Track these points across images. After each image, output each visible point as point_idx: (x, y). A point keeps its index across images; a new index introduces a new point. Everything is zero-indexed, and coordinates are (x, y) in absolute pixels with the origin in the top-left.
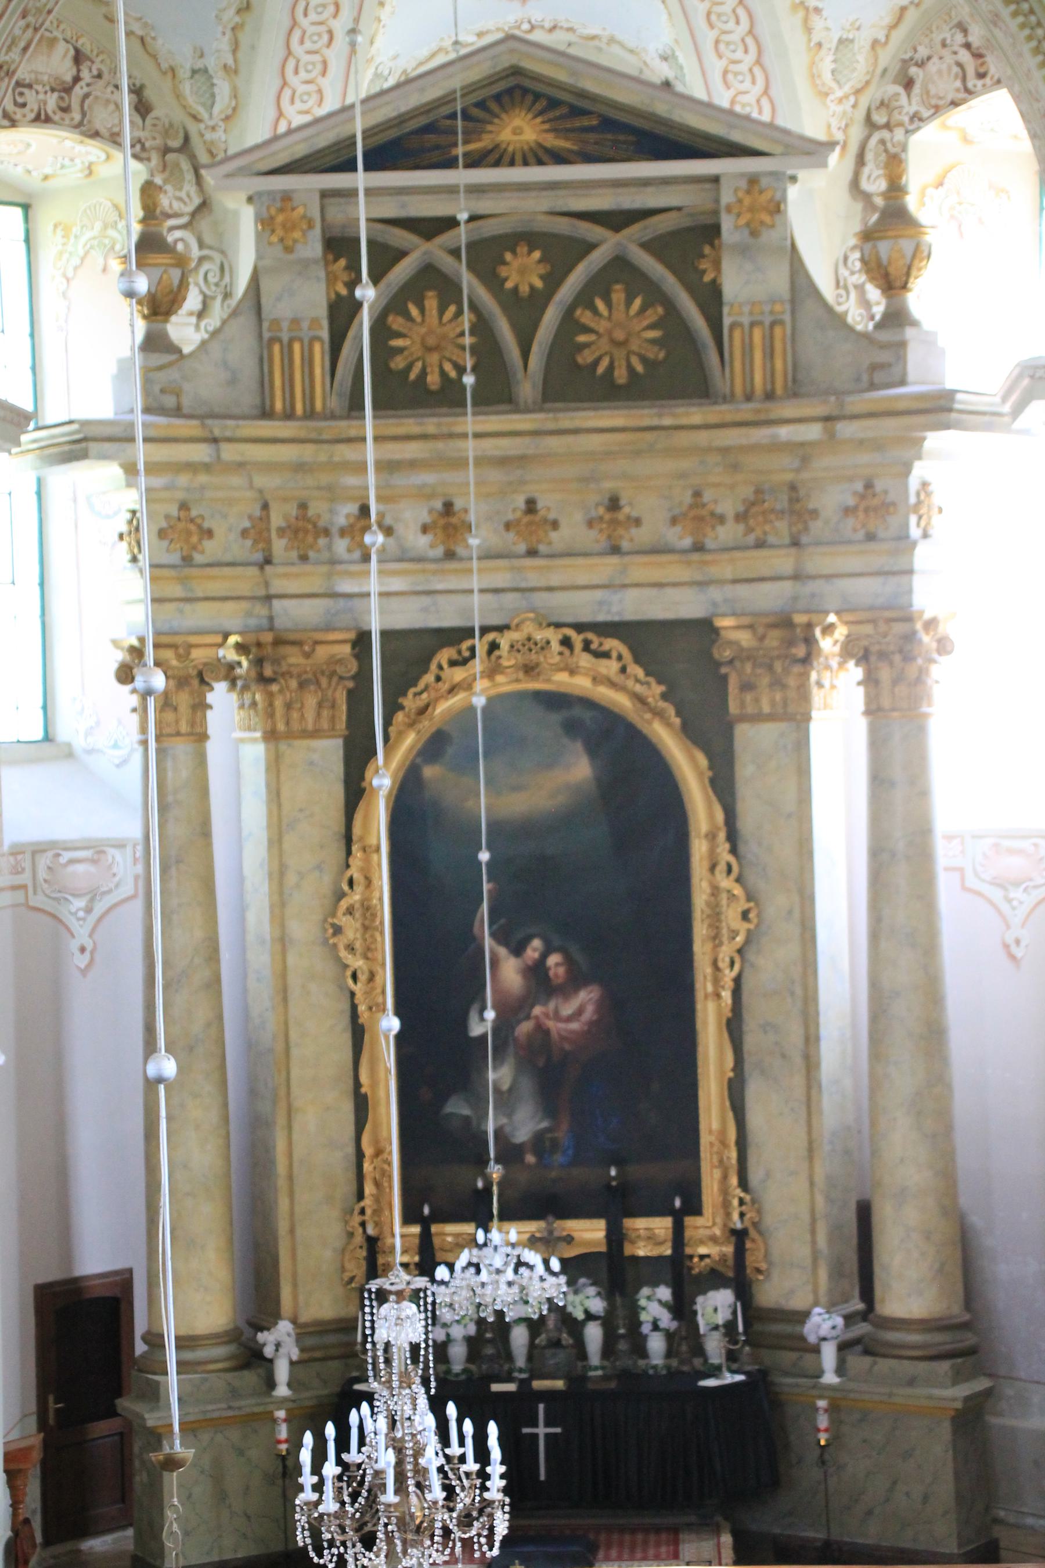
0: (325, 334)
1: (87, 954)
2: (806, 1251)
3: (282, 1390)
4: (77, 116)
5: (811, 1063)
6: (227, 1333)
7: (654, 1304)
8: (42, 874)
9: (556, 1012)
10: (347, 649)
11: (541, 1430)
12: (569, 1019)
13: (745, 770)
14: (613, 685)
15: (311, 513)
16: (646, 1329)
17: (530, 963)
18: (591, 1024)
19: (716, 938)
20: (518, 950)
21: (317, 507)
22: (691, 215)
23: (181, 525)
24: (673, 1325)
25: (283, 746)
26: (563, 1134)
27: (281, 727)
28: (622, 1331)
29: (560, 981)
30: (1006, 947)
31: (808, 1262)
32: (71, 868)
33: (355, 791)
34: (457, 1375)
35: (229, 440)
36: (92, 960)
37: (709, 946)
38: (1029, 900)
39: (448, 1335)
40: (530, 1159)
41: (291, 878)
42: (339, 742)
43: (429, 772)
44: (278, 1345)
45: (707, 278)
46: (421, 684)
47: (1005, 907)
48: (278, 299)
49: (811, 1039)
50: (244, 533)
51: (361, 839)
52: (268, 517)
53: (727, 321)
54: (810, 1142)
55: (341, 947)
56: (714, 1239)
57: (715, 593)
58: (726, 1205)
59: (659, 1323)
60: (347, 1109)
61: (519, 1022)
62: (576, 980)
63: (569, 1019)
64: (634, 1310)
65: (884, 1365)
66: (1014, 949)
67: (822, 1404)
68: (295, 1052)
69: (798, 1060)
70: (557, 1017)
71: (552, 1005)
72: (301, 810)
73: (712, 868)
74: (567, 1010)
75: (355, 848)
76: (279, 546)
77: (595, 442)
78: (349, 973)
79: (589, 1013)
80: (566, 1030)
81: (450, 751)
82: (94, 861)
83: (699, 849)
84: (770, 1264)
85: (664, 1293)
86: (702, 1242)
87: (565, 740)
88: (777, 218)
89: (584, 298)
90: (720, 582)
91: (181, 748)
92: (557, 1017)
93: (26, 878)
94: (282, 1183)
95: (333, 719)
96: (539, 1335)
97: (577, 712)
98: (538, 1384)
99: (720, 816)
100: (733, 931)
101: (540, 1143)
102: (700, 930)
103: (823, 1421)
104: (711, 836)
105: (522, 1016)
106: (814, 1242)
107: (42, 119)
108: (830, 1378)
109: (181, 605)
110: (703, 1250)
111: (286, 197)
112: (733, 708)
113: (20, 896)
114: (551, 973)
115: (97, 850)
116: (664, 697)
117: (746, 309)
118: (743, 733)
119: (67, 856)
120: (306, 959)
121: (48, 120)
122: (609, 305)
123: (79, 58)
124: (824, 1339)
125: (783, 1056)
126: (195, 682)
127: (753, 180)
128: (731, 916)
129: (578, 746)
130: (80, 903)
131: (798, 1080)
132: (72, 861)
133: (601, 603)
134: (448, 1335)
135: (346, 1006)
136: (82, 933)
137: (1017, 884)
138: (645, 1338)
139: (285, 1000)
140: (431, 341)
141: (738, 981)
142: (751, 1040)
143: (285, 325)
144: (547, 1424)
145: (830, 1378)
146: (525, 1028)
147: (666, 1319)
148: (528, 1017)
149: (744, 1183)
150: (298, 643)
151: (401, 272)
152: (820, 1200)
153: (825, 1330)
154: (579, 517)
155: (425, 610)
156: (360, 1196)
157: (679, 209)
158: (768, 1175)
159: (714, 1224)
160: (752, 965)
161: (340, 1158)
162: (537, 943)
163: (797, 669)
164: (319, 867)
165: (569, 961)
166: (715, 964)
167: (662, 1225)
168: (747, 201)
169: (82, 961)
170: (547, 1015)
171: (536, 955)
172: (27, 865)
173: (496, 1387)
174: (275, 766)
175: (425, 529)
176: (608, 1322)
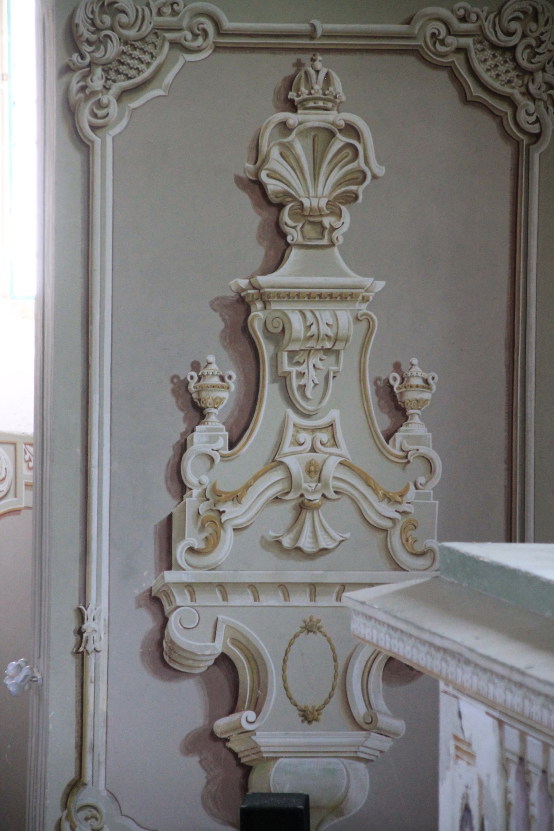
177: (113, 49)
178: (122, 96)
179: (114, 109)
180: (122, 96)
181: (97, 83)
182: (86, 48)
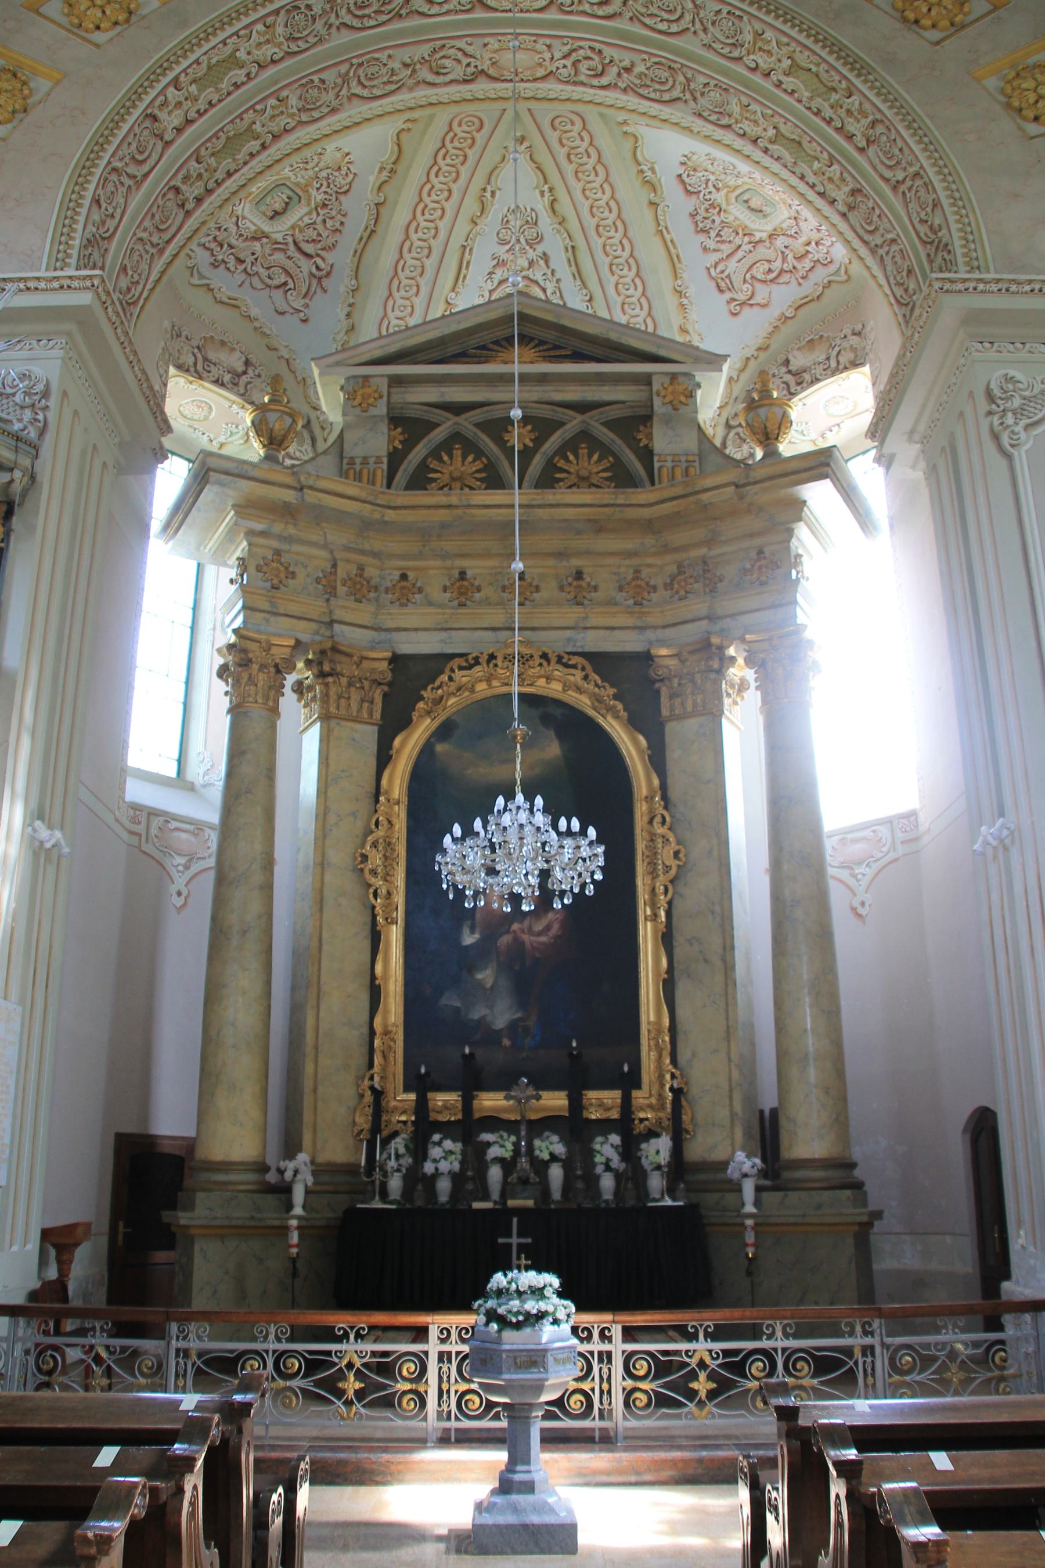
0: (385, 466)
1: (183, 897)
2: (726, 1112)
3: (298, 1210)
4: (242, 391)
5: (728, 966)
6: (255, 1163)
7: (607, 1149)
8: (154, 831)
9: (530, 929)
10: (384, 665)
11: (515, 1240)
13: (674, 754)
14: (579, 689)
15: (366, 575)
16: (599, 1169)
18: (557, 938)
19: (653, 873)
21: (371, 572)
22: (631, 407)
23: (275, 565)
24: (622, 1166)
25: (333, 723)
26: (532, 1023)
27: (333, 709)
28: (579, 1172)
30: (853, 909)
31: (727, 1122)
32: (176, 834)
33: (384, 758)
35: (311, 488)
36: (185, 904)
37: (648, 880)
38: (870, 872)
39: (437, 1169)
40: (506, 1042)
41: (332, 819)
42: (376, 728)
43: (440, 748)
44: (296, 1172)
45: (644, 442)
46: (437, 683)
47: (852, 882)
48: (356, 445)
49: (728, 947)
50: (318, 581)
51: (387, 792)
52: (336, 573)
53: (656, 465)
54: (728, 1027)
55: (367, 871)
56: (651, 1106)
57: (650, 635)
58: (661, 1077)
60: (365, 997)
64: (590, 1153)
65: (793, 1197)
66: (860, 910)
67: (749, 1222)
68: (326, 947)
69: (719, 963)
70: (530, 931)
73: (651, 821)
74: (539, 927)
75: (382, 799)
76: (342, 590)
77: (570, 513)
78: (371, 890)
82: (193, 834)
83: (641, 810)
84: (695, 1125)
85: (615, 1139)
86: (641, 1109)
88: (690, 400)
89: (561, 452)
90: (655, 627)
91: (257, 711)
92: (530, 931)
93: (141, 828)
94: (309, 1050)
95: (371, 713)
96: (511, 1174)
98: (511, 1203)
99: (656, 782)
102: (641, 868)
103: (750, 1237)
104: (649, 799)
106: (731, 1105)
107: (218, 382)
108: (749, 1208)
109: (268, 616)
110: (642, 1115)
111: (366, 378)
112: (665, 712)
113: (135, 840)
115: (198, 827)
116: (616, 697)
117: (669, 458)
118: (671, 728)
119: (174, 824)
120: (340, 880)
121: (223, 385)
122: (577, 457)
123: (247, 363)
124: (745, 1175)
125: (706, 961)
126: (272, 670)
127: (673, 377)
128: (666, 855)
129: (552, 733)
130: (180, 860)
131: (719, 978)
132: (177, 829)
133: (569, 640)
134: (437, 1169)
135: (369, 920)
136: (180, 882)
137: (859, 863)
138: (598, 1178)
139: (321, 910)
140: (456, 475)
141: (670, 903)
142: (678, 952)
143: (358, 461)
144: (519, 1235)
145: (749, 1208)
146: (505, 940)
147: (616, 1162)
148: (508, 932)
149: (674, 1062)
150: (350, 655)
151: (438, 435)
152: (736, 1075)
153: (747, 1167)
154: (554, 584)
155: (442, 641)
156: (371, 1065)
157: (623, 402)
158: (694, 1055)
159: (651, 1095)
160: (681, 896)
161: (355, 1036)
163: (713, 676)
164: (354, 814)
166: (653, 891)
167: (612, 1097)
168: (670, 389)
169: (179, 902)
170: (523, 931)
172: (144, 820)
173: (477, 1205)
174: (325, 740)
175: (445, 589)
176: (567, 1165)
177: (1017, 402)
178: (1027, 427)
179: (1023, 435)
180: (1027, 427)
181: (1010, 419)
182: (1000, 402)
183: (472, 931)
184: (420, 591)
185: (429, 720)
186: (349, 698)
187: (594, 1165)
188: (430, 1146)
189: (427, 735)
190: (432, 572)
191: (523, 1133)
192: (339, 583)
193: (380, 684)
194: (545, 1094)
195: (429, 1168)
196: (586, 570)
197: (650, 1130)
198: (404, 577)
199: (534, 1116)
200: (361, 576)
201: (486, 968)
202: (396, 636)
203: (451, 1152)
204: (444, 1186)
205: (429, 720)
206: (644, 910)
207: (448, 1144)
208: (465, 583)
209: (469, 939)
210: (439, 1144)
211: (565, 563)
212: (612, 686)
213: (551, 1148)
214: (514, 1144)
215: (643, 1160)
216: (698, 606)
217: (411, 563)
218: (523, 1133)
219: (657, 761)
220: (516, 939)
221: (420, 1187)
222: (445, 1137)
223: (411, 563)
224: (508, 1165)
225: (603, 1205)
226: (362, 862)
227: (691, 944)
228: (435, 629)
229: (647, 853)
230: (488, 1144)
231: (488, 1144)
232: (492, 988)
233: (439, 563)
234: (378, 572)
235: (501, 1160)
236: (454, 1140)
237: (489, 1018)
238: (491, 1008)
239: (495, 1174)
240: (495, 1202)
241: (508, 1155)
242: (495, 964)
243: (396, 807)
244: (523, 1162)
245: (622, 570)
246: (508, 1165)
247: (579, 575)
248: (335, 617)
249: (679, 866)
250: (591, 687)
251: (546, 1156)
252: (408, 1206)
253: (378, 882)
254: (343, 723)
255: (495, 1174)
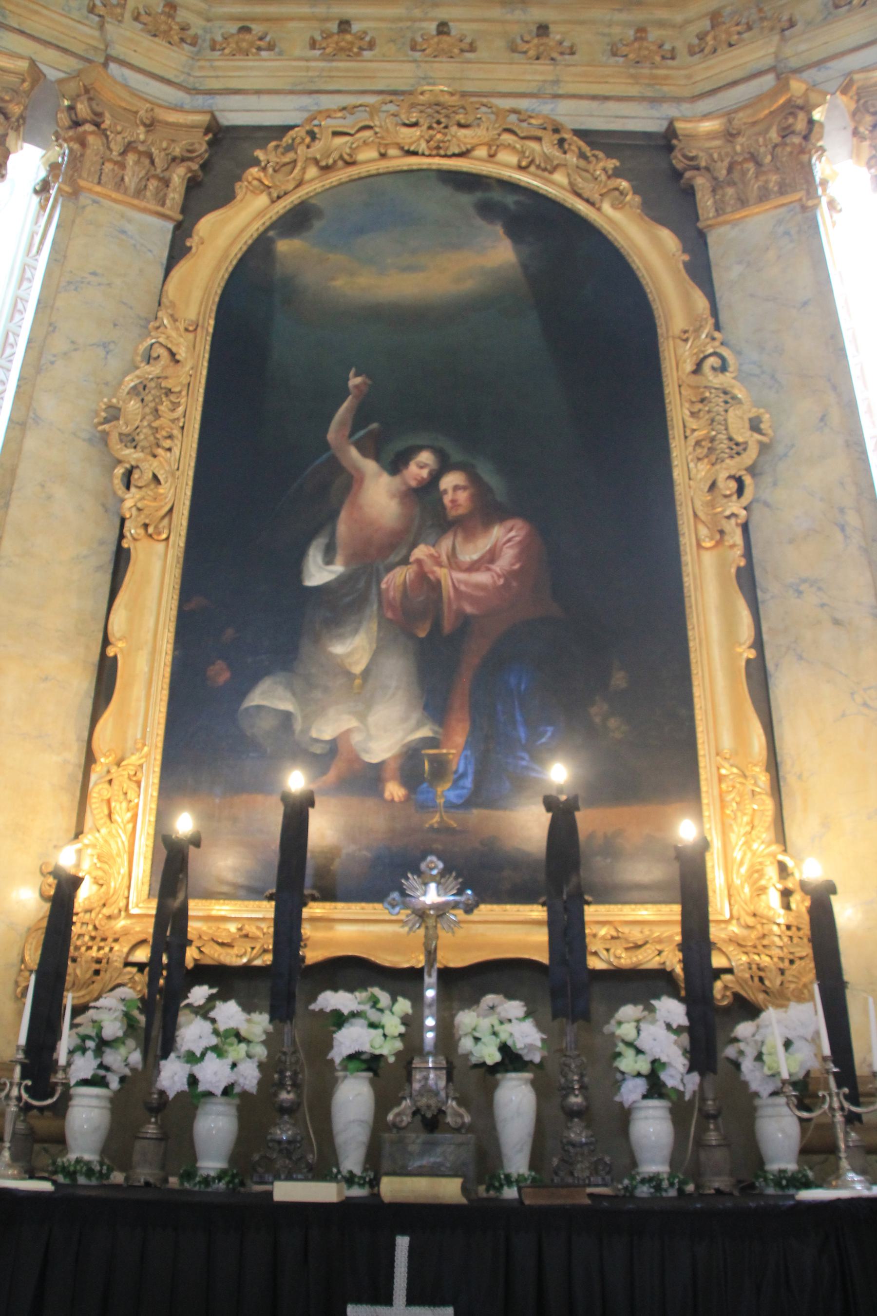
7: (654, 1033)
9: (453, 554)
12: (473, 567)
16: (632, 1091)
17: (413, 484)
18: (510, 576)
20: (396, 465)
29: (461, 511)
34: (207, 1181)
39: (193, 1081)
40: (394, 790)
41: (59, 344)
42: (170, 226)
43: (283, 246)
55: (114, 438)
57: (669, 110)
59: (664, 1076)
61: (389, 568)
62: (487, 511)
63: (473, 567)
70: (453, 562)
71: (446, 544)
72: (94, 274)
73: (698, 369)
74: (470, 553)
78: (119, 471)
79: (507, 559)
80: (466, 583)
81: (318, 225)
85: (672, 1009)
87: (479, 222)
90: (678, 100)
92: (453, 562)
97: (497, 195)
98: (392, 1188)
99: (701, 303)
100: (737, 444)
101: (415, 767)
105: (394, 558)
114: (447, 499)
116: (617, 173)
125: (837, 622)
129: (499, 229)
134: (193, 1081)
146: (397, 578)
147: (678, 1074)
148: (405, 561)
154: (500, 43)
160: (766, 504)
162: (425, 457)
165: (475, 479)
170: (438, 562)
171: (425, 473)
173: (286, 1191)
175: (313, 44)
183: (329, 559)
184: (271, 47)
185: (263, 200)
186: (122, 166)
187: (617, 1079)
188: (183, 1017)
189: (257, 227)
190: (292, 25)
191: (430, 993)
192: (128, 15)
193: (183, 160)
194: (485, 910)
195: (172, 1075)
196: (552, 28)
197: (737, 996)
198: (245, 29)
199: (457, 961)
200: (171, 16)
201: (356, 631)
202: (220, 102)
203: (239, 1038)
204: (215, 1131)
205: (263, 200)
206: (692, 534)
207: (229, 1013)
208: (348, 37)
209: (319, 573)
210: (204, 1011)
211: (518, 14)
212: (609, 156)
213: (504, 1033)
214: (406, 1021)
215: (747, 1065)
216: (758, 52)
217: (259, 10)
218: (430, 993)
219: (700, 270)
220: (422, 576)
221: (151, 1130)
222: (223, 996)
223: (259, 10)
224: (387, 1076)
225: (644, 1191)
226: (106, 421)
227: (800, 593)
228: (292, 92)
229: (692, 424)
230: (339, 1019)
231: (339, 1019)
232: (366, 673)
233: (306, 10)
234: (202, 23)
235: (370, 1063)
236: (248, 1008)
237: (356, 738)
238: (362, 717)
239: (353, 1099)
240: (350, 1180)
241: (389, 1049)
242: (374, 626)
243: (191, 336)
244: (430, 1074)
245: (616, 30)
246: (387, 1076)
247: (543, 29)
248: (113, 52)
249: (764, 448)
250: (572, 159)
251: (493, 1056)
252: (118, 1177)
253: (131, 455)
254: (106, 203)
255: (353, 1099)
